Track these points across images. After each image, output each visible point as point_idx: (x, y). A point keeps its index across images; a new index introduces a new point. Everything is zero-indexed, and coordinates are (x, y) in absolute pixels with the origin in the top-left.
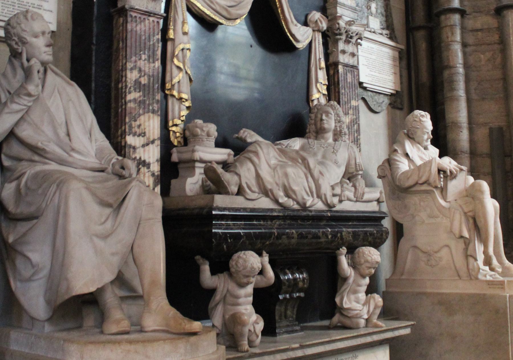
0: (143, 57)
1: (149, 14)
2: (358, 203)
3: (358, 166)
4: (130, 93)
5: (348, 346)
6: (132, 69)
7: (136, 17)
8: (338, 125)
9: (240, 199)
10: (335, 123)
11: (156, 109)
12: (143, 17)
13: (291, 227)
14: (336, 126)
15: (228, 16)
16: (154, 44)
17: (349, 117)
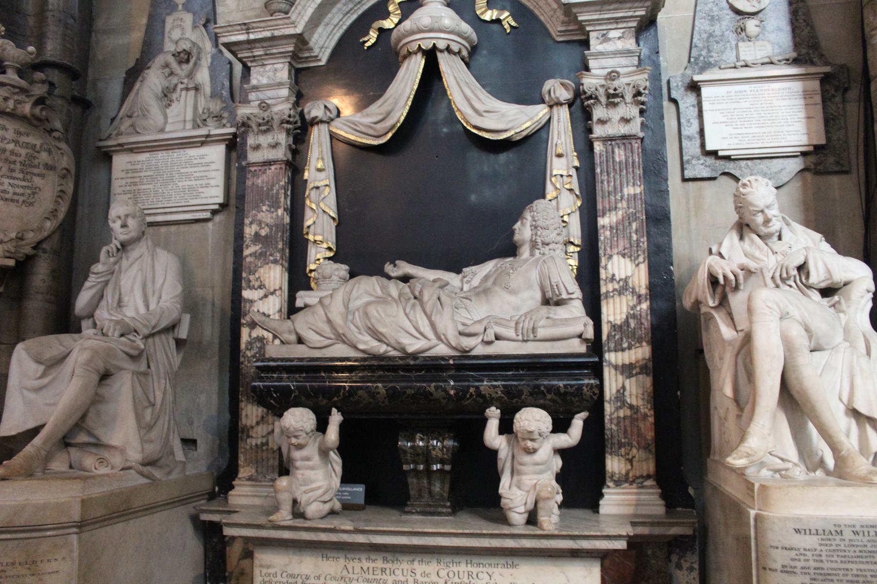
0: (264, 208)
1: (268, 163)
2: (529, 343)
3: (555, 287)
4: (247, 247)
5: (402, 543)
6: (251, 223)
7: (255, 171)
8: (534, 232)
9: (301, 347)
10: (532, 230)
11: (278, 258)
12: (263, 168)
13: (380, 379)
14: (532, 235)
15: (376, 134)
16: (277, 193)
17: (616, 213)
